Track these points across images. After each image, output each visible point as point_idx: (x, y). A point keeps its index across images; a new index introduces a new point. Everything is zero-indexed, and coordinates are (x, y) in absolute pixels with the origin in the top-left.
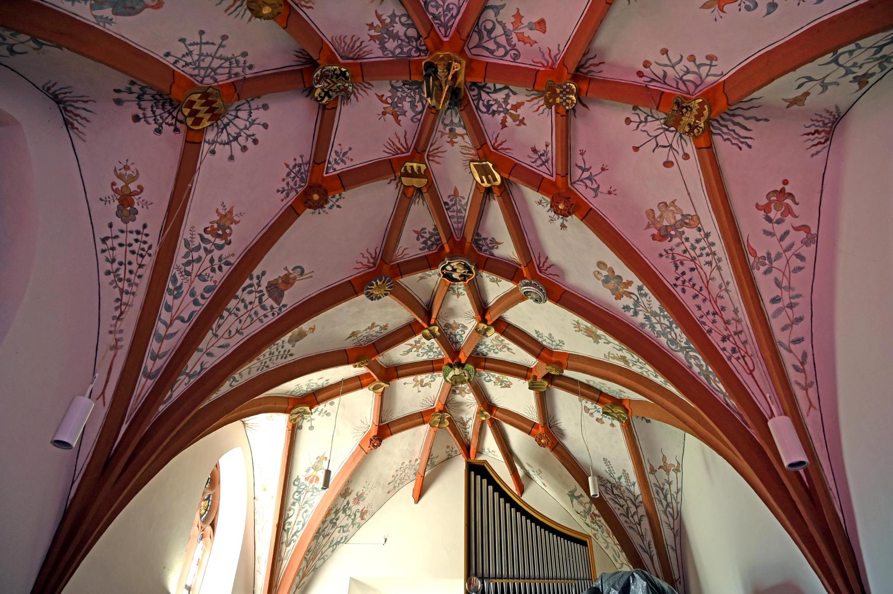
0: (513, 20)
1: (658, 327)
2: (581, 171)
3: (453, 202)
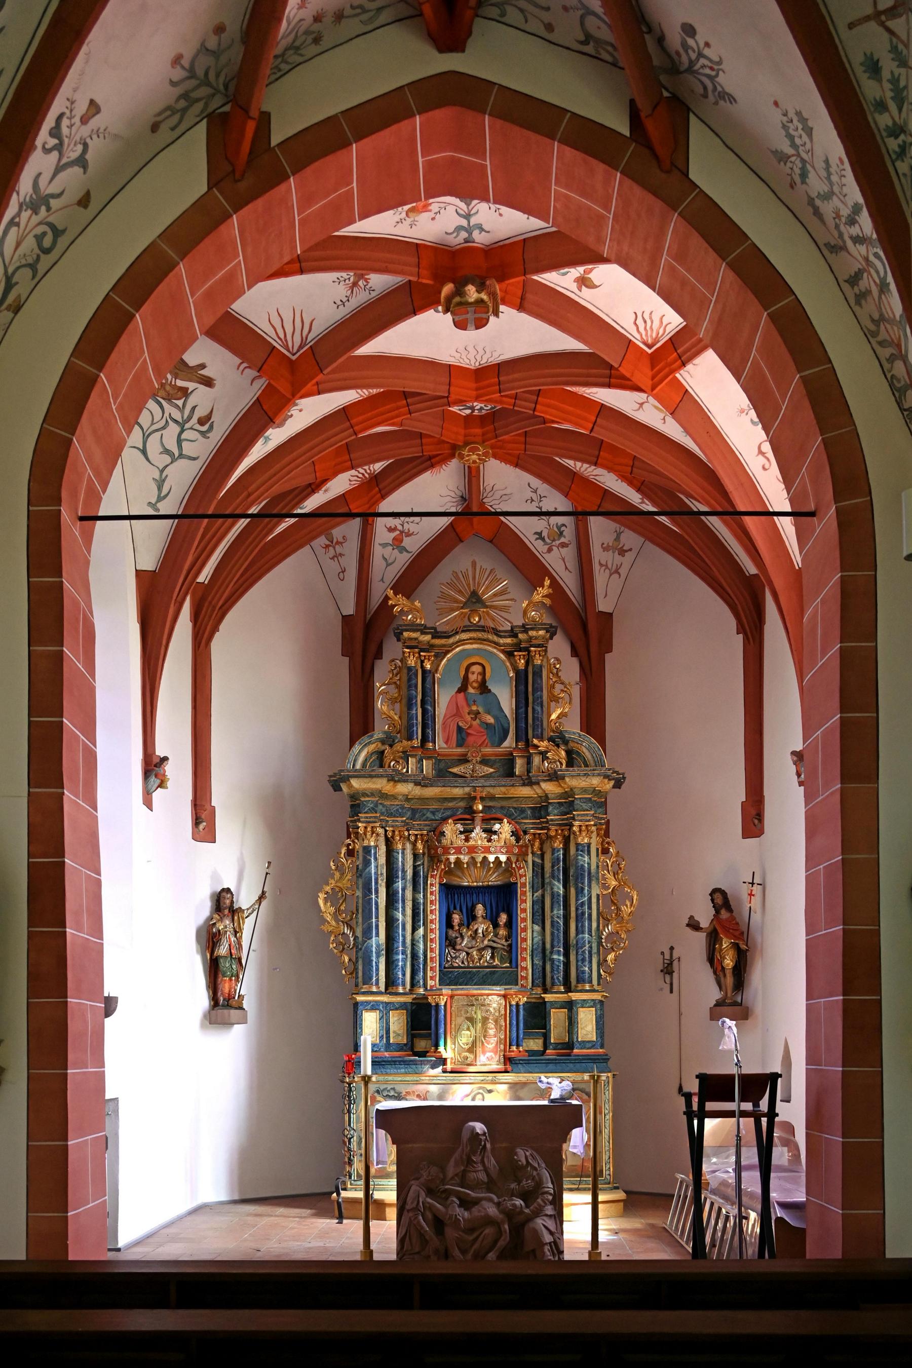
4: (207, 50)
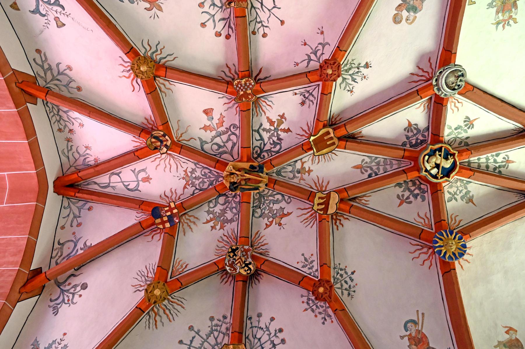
0: (208, 131)
2: (312, 62)
3: (368, 169)
4: (70, 82)
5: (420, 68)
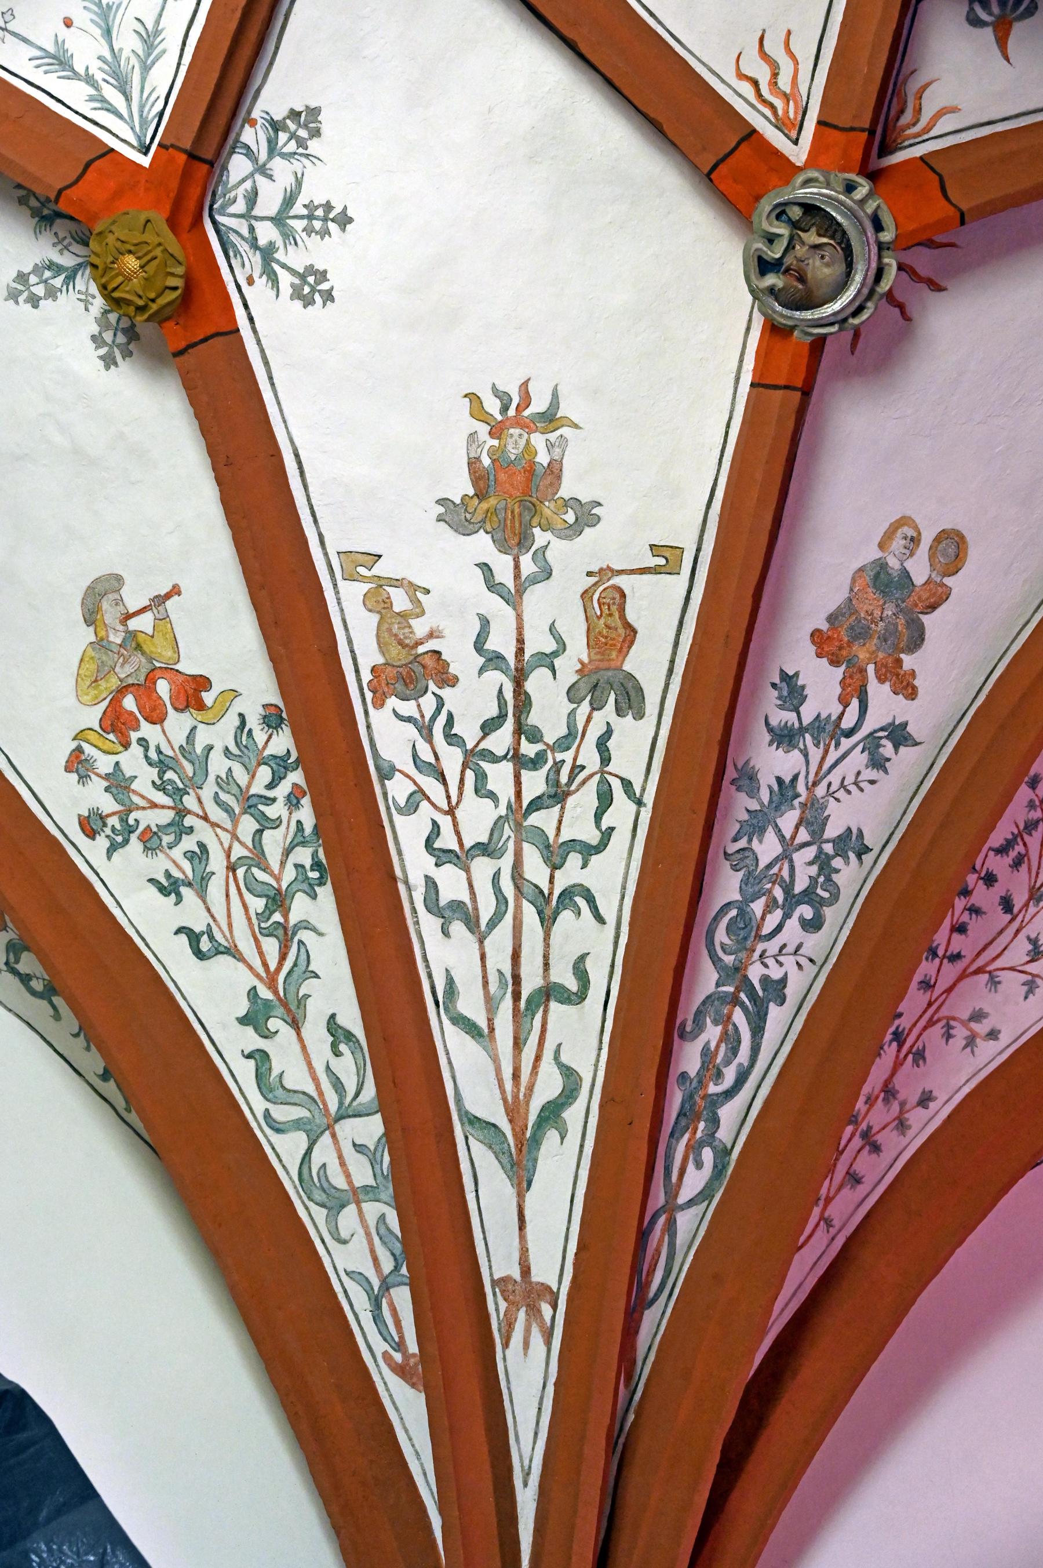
1: (767, 848)
5: (897, 310)
